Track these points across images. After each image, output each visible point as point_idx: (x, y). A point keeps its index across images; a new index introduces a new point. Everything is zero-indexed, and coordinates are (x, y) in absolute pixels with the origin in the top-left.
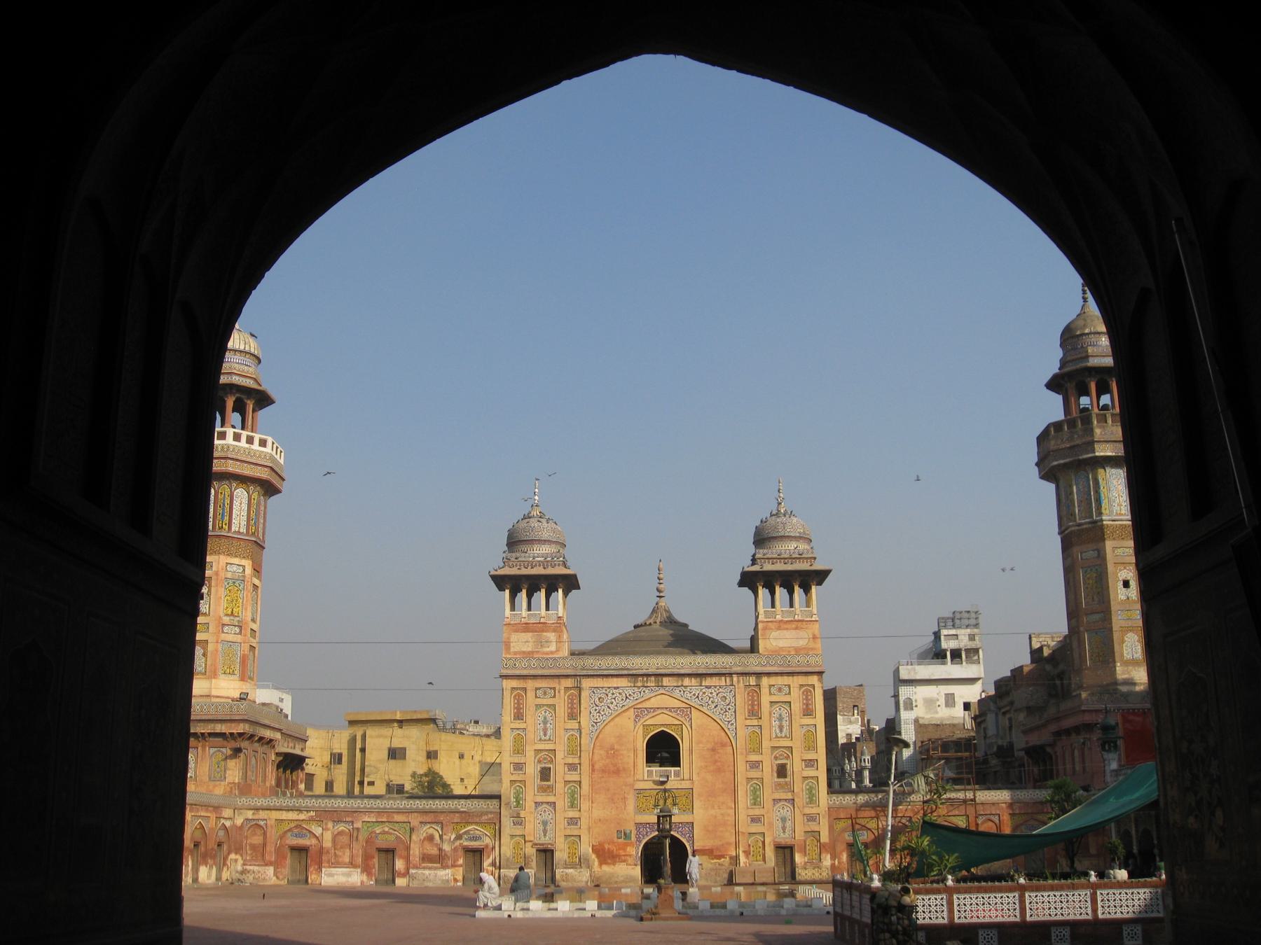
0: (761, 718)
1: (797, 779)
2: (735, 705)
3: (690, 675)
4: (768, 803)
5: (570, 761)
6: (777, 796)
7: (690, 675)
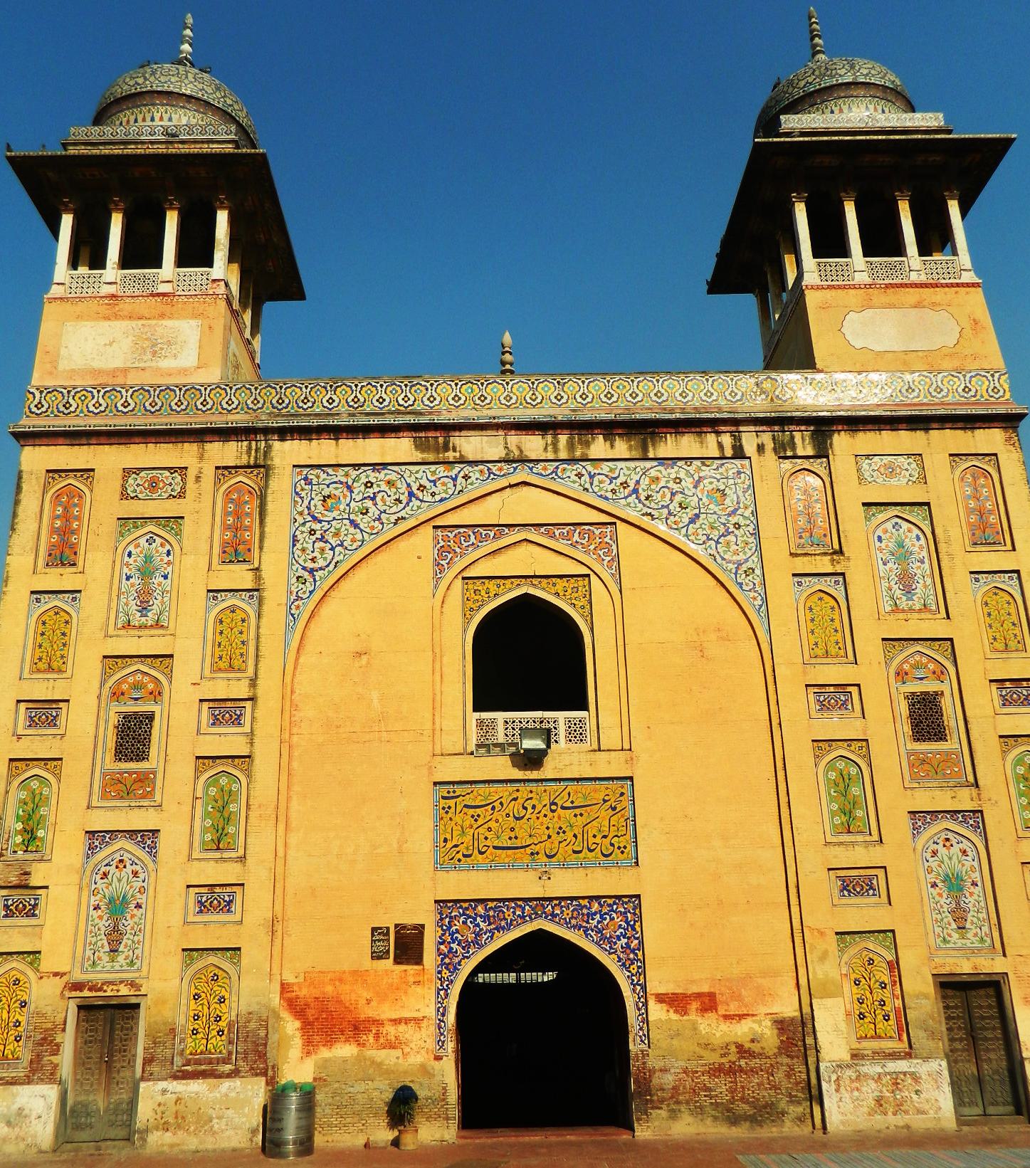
0: (841, 552)
1: (987, 748)
2: (755, 513)
3: (610, 428)
4: (896, 825)
5: (221, 689)
6: (926, 800)
7: (610, 428)
